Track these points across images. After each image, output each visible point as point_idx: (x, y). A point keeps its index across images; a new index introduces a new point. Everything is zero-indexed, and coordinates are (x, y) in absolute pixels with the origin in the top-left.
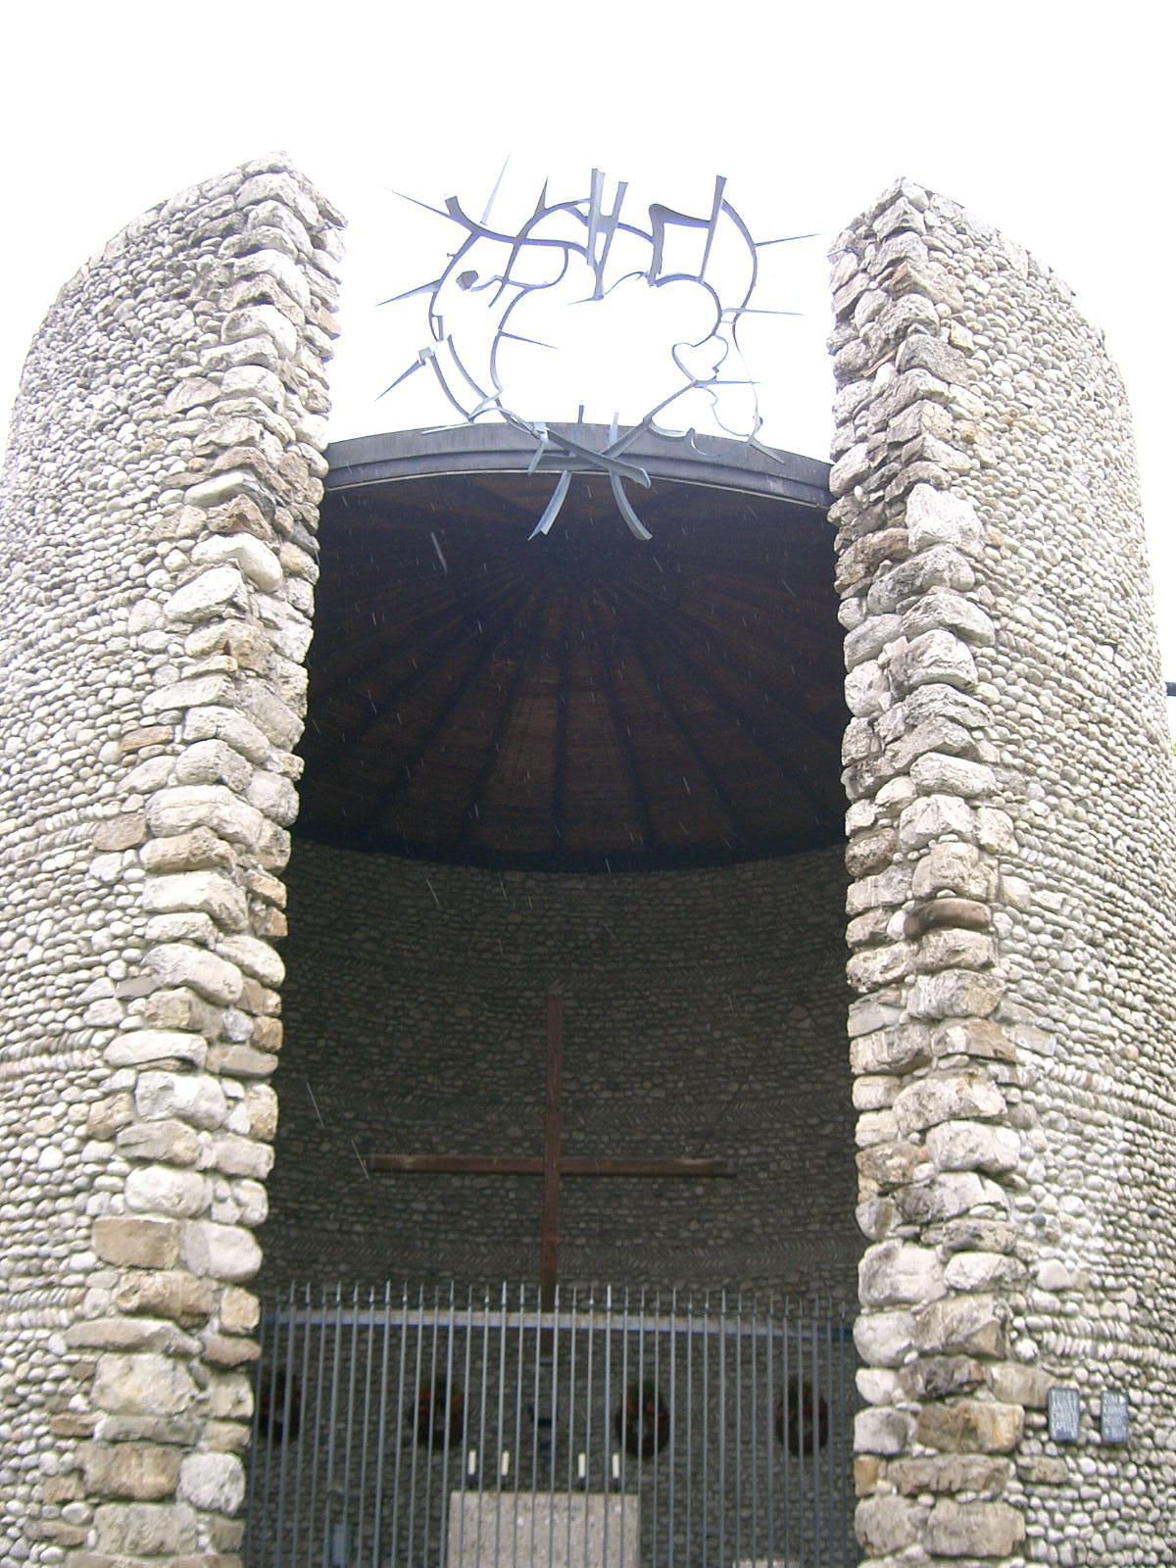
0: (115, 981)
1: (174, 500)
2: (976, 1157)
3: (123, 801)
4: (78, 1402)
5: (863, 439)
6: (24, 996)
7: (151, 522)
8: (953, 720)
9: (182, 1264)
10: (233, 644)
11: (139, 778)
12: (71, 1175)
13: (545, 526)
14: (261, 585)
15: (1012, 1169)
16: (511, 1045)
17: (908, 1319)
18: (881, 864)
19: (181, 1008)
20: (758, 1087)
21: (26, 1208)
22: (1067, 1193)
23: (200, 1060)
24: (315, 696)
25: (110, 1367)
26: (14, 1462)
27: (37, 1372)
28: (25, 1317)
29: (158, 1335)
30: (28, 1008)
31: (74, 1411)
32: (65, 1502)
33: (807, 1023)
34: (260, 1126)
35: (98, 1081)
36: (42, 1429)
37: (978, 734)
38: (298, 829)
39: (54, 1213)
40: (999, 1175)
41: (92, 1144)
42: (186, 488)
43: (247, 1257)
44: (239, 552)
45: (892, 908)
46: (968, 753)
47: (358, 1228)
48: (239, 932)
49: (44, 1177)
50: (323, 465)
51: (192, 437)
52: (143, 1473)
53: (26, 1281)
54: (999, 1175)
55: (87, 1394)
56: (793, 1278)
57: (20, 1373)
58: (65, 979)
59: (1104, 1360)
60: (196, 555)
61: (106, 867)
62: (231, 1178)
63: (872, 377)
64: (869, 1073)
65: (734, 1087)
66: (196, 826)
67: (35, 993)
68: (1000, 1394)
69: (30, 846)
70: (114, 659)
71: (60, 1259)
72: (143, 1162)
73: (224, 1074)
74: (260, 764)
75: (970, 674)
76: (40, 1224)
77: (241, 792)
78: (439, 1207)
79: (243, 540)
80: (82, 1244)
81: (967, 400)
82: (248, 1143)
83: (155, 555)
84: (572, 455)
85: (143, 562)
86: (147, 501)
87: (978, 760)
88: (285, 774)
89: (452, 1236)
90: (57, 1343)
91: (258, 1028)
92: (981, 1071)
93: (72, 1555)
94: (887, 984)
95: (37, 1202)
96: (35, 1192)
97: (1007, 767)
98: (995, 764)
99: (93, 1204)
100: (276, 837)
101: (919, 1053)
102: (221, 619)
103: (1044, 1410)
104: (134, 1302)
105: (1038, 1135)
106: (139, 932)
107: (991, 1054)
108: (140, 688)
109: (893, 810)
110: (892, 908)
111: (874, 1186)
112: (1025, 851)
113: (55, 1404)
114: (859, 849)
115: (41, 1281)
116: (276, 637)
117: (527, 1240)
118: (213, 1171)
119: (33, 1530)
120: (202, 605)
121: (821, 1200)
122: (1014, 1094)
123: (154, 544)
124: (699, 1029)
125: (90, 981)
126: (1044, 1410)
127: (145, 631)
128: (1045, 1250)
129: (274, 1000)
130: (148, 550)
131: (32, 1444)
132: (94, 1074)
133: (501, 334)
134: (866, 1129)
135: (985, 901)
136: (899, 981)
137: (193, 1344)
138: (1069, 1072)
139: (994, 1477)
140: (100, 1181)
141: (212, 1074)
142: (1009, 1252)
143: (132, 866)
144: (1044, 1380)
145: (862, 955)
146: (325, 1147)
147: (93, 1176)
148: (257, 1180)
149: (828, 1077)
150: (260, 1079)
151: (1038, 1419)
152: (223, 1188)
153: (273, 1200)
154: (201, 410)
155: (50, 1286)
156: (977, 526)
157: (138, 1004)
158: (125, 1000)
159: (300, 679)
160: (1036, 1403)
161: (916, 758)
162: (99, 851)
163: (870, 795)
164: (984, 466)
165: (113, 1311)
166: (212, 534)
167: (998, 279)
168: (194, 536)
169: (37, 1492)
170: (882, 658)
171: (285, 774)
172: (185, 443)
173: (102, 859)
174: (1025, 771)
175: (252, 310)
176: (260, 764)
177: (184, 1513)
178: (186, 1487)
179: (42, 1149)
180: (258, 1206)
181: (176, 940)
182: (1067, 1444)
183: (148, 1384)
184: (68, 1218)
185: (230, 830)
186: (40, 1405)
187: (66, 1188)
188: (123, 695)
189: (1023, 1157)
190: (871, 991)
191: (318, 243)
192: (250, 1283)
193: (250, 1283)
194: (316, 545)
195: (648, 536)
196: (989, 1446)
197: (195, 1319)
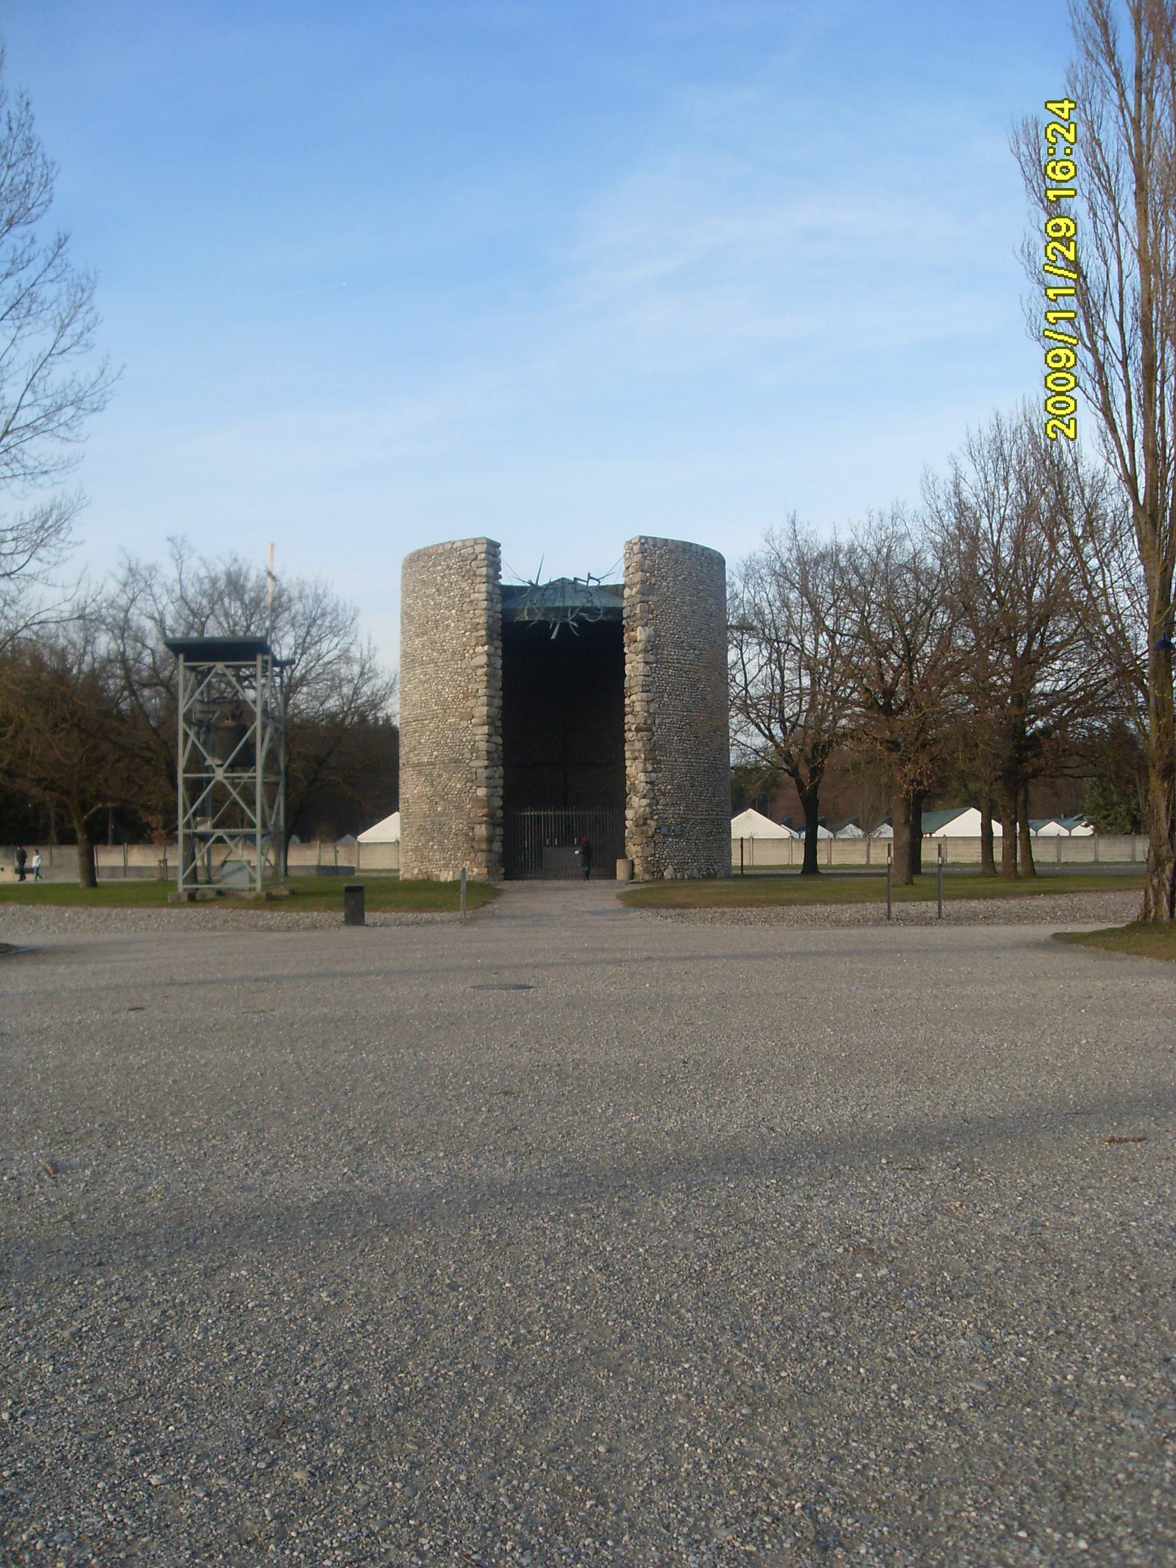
25: (477, 827)
38: (502, 708)
43: (501, 803)
70: (459, 675)
114: (627, 709)
180: (501, 792)
182: (665, 835)
192: (501, 808)
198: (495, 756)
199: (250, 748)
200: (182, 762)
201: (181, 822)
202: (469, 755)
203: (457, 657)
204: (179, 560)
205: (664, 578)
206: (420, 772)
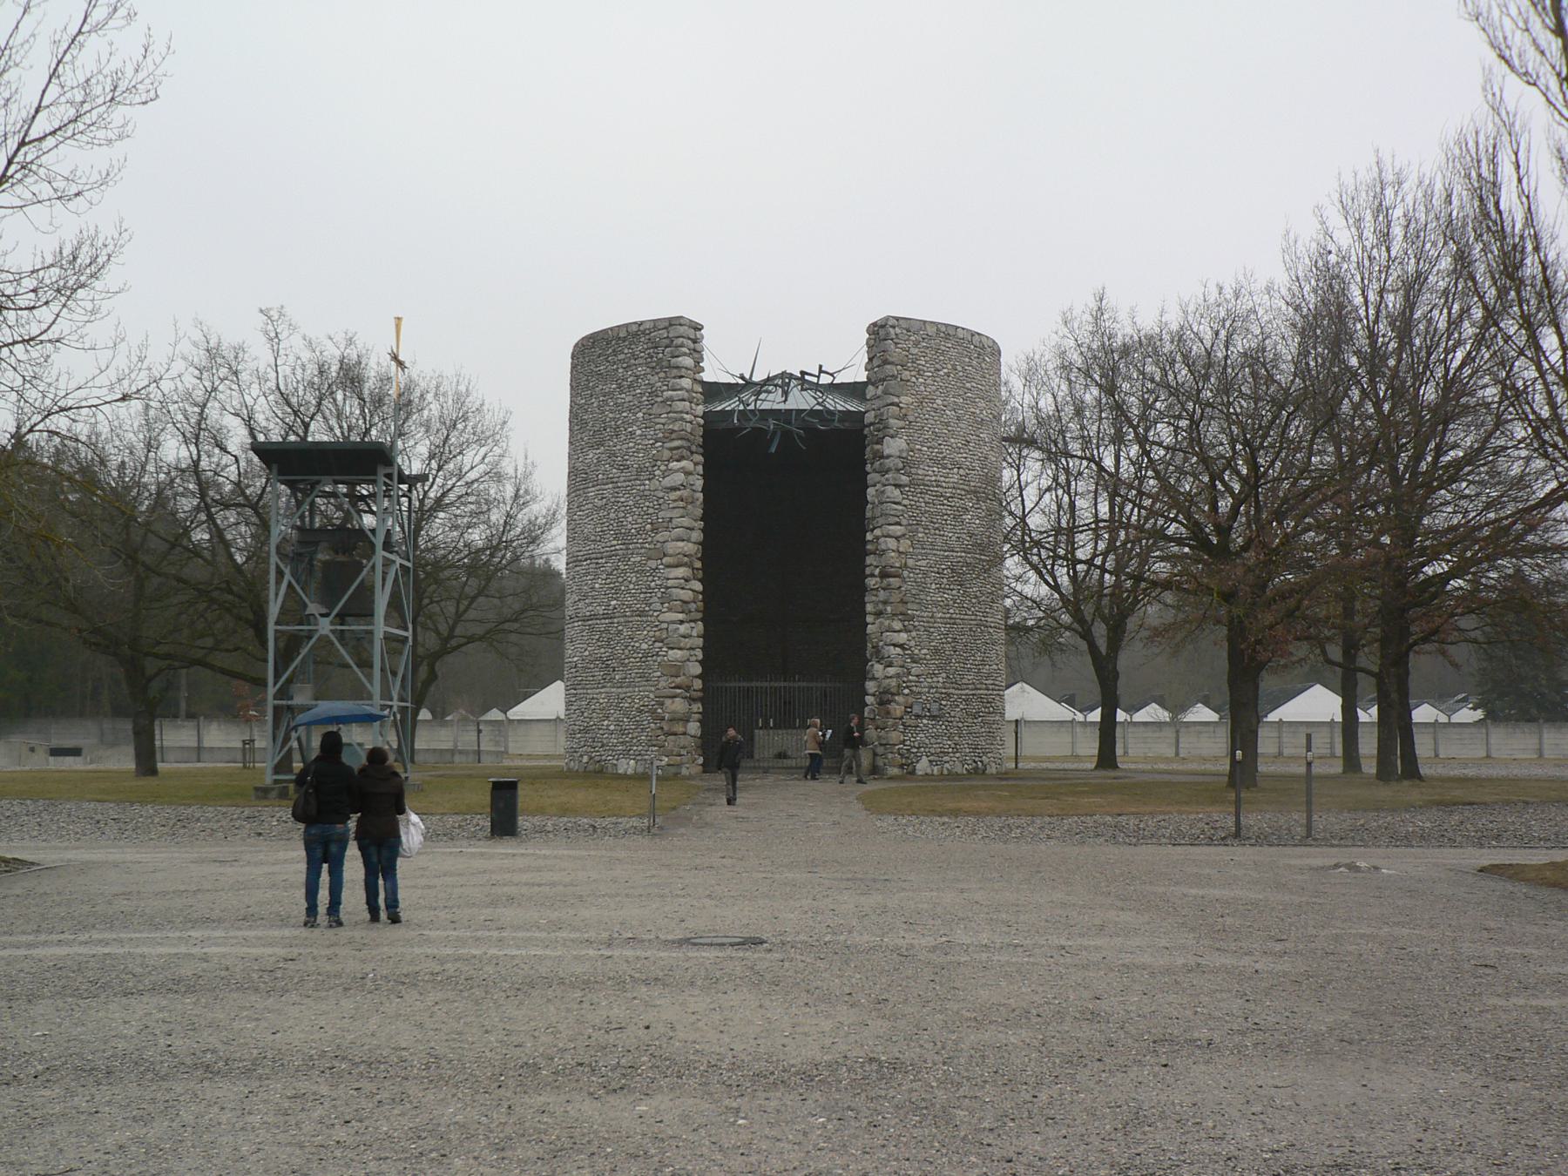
11: (659, 537)
13: (773, 450)
14: (687, 473)
25: (668, 702)
40: (901, 646)
43: (698, 670)
50: (702, 421)
52: (679, 728)
54: (901, 646)
74: (692, 529)
77: (688, 540)
79: (684, 463)
109: (878, 538)
114: (869, 547)
139: (895, 725)
144: (911, 700)
176: (692, 529)
180: (699, 654)
182: (918, 716)
183: (678, 705)
191: (695, 341)
197: (688, 688)
198: (693, 606)
199: (366, 592)
200: (274, 610)
201: (271, 690)
202: (658, 606)
203: (644, 475)
204: (274, 339)
205: (920, 373)
206: (592, 629)
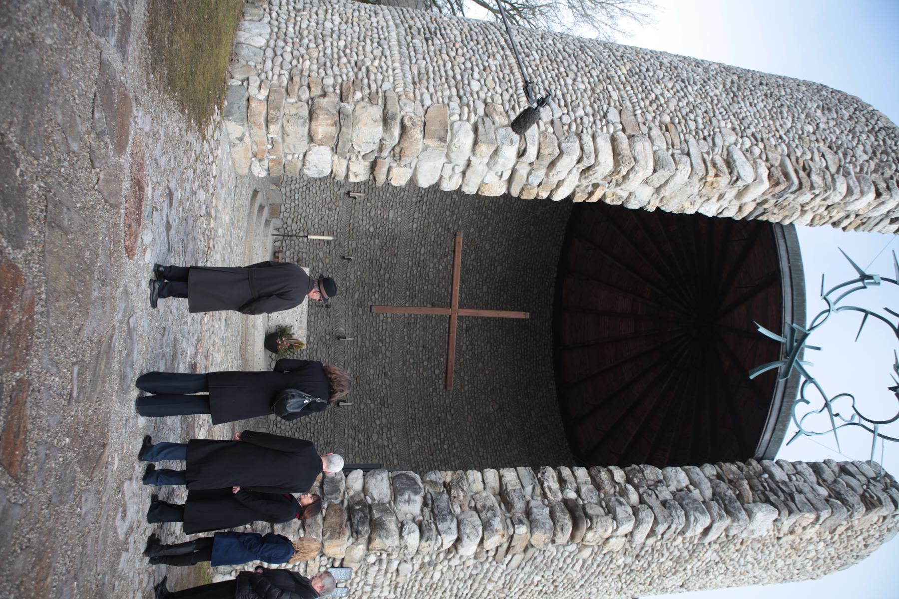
0: (560, 118)
1: (783, 151)
2: (465, 537)
3: (644, 124)
4: (359, 95)
5: (790, 480)
6: (549, 75)
7: (772, 139)
8: (669, 527)
9: (426, 148)
10: (718, 179)
11: (655, 132)
12: (468, 95)
13: (762, 330)
15: (457, 553)
16: (485, 289)
17: (386, 500)
18: (598, 486)
19: (550, 150)
20: (466, 388)
21: (450, 73)
22: (442, 573)
23: (524, 159)
24: (682, 217)
25: (376, 112)
26: (328, 64)
27: (372, 77)
28: (398, 71)
29: (392, 135)
30: (544, 77)
31: (354, 93)
32: (309, 87)
33: (491, 410)
34: (487, 187)
35: (513, 108)
36: (345, 78)
37: (659, 537)
38: (621, 208)
39: (449, 87)
41: (483, 106)
42: (788, 156)
43: (424, 182)
44: (762, 182)
45: (578, 491)
46: (652, 533)
47: (415, 225)
48: (580, 180)
49: (466, 82)
51: (812, 159)
52: (323, 127)
53: (416, 72)
55: (363, 99)
56: (390, 401)
57: (371, 68)
58: (559, 93)
59: (363, 588)
60: (759, 161)
61: (613, 115)
62: (464, 173)
63: (819, 484)
64: (501, 477)
65: (466, 378)
66: (635, 159)
67: (551, 80)
68: (349, 549)
69: (616, 79)
71: (427, 88)
72: (476, 130)
73: (514, 171)
75: (688, 534)
76: (444, 79)
77: (646, 182)
78: (422, 258)
80: (435, 100)
81: (811, 532)
82: (479, 182)
83: (757, 141)
84: (795, 344)
85: (753, 135)
86: (781, 137)
87: (648, 536)
88: (649, 203)
89: (410, 263)
90: (387, 86)
91: (533, 188)
92: (505, 539)
93: (283, 90)
94: (543, 489)
95: (454, 77)
96: (459, 77)
97: (642, 548)
98: (644, 544)
99: (455, 104)
100: (620, 198)
101: (512, 506)
102: (730, 173)
103: (341, 566)
104: (408, 123)
105: (471, 562)
106: (585, 131)
107: (513, 544)
108: (697, 133)
110: (578, 491)
111: (448, 480)
112: (602, 556)
113: (356, 84)
115: (416, 79)
116: (714, 200)
117: (408, 293)
118: (469, 164)
119: (295, 71)
120: (737, 163)
121: (421, 414)
122: (492, 553)
123: (762, 140)
124: (490, 364)
125: (559, 106)
126: (341, 566)
127: (722, 136)
128: (417, 567)
129: (544, 195)
130: (759, 136)
131: (337, 73)
132: (517, 106)
133: (867, 313)
134: (474, 475)
135: (582, 540)
136: (544, 495)
137: (385, 154)
138: (498, 574)
140: (466, 109)
141: (515, 166)
142: (418, 552)
143: (615, 127)
145: (555, 475)
146: (448, 213)
147: (468, 106)
148: (461, 186)
149: (470, 418)
150: (508, 189)
151: (337, 564)
152: (459, 170)
153: (450, 193)
154: (824, 164)
155: (414, 83)
156: (753, 537)
157: (551, 130)
158: (552, 123)
159: (690, 211)
160: (345, 563)
161: (650, 507)
162: (620, 112)
163: (629, 481)
164: (779, 538)
165: (403, 113)
166: (769, 169)
167: (861, 545)
168: (767, 160)
169: (314, 74)
170: (691, 487)
171: (649, 203)
172: (809, 156)
173: (616, 112)
174: (637, 556)
175: (873, 189)
176: (658, 190)
177: (303, 146)
178: (316, 149)
179: (479, 81)
180: (448, 186)
181: (582, 149)
183: (367, 132)
184: (447, 93)
185: (631, 176)
186: (357, 78)
187: (462, 92)
188: (692, 125)
189: (461, 557)
190: (539, 480)
193: (412, 181)
194: (751, 219)
195: (752, 377)
196: (326, 544)
197: (398, 154)
